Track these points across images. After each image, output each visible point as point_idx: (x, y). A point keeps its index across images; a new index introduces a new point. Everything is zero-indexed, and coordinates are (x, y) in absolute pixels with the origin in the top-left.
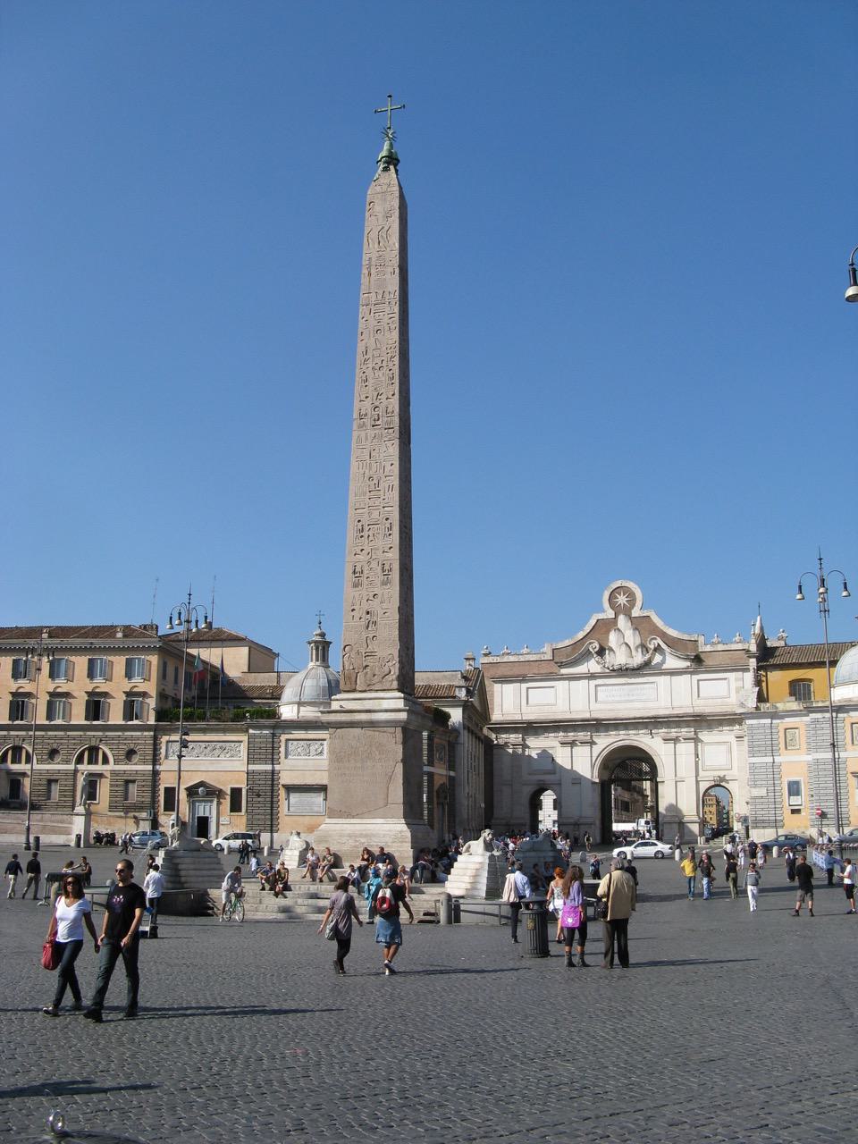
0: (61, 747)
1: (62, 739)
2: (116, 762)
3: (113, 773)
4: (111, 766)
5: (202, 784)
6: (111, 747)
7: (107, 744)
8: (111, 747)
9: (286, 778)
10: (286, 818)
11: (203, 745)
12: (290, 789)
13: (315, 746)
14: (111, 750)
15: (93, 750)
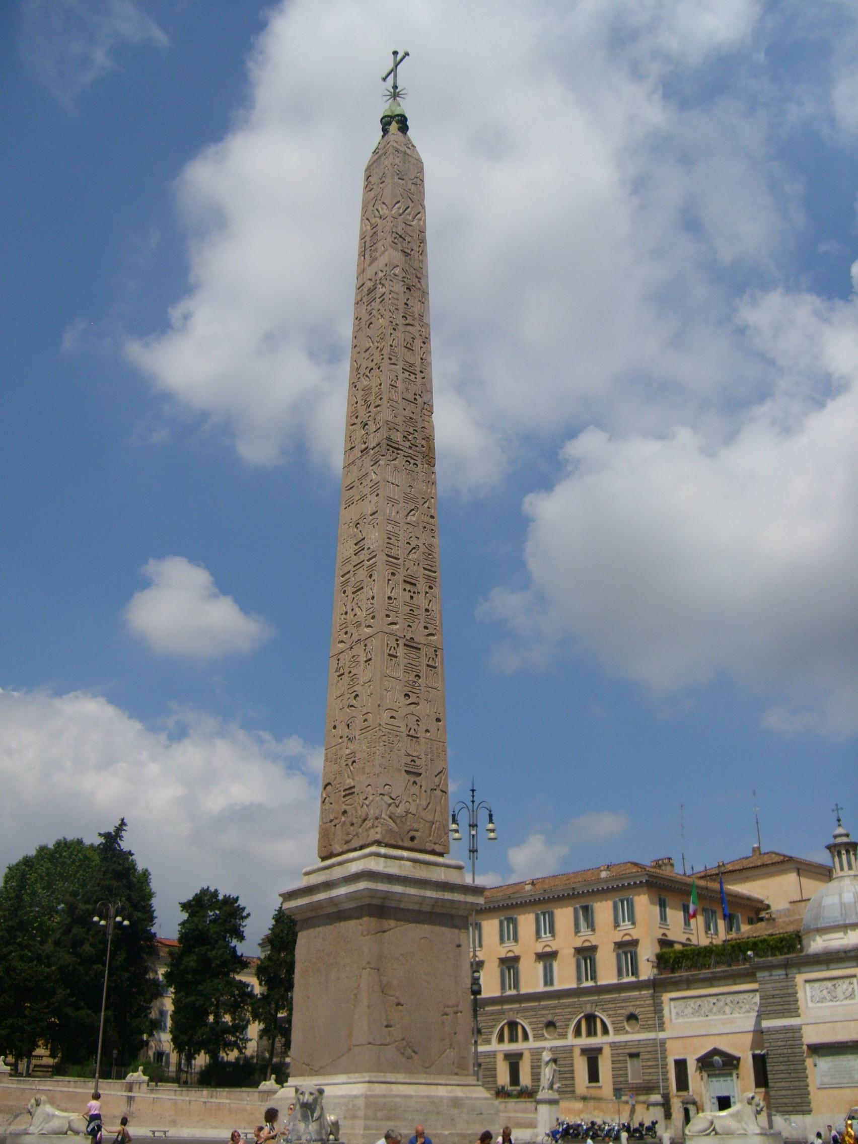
0: (556, 1018)
1: (555, 1007)
2: (618, 1031)
3: (613, 1045)
4: (612, 1037)
5: (716, 1052)
6: (610, 1013)
7: (604, 1010)
8: (610, 1013)
9: (811, 1036)
10: (820, 1093)
11: (713, 1000)
12: (818, 1050)
13: (844, 986)
14: (609, 1016)
15: (591, 1019)
